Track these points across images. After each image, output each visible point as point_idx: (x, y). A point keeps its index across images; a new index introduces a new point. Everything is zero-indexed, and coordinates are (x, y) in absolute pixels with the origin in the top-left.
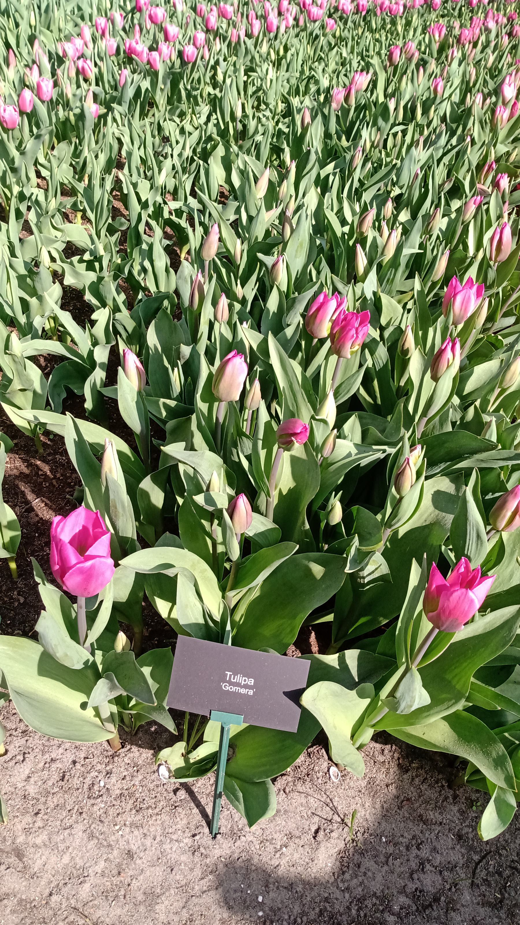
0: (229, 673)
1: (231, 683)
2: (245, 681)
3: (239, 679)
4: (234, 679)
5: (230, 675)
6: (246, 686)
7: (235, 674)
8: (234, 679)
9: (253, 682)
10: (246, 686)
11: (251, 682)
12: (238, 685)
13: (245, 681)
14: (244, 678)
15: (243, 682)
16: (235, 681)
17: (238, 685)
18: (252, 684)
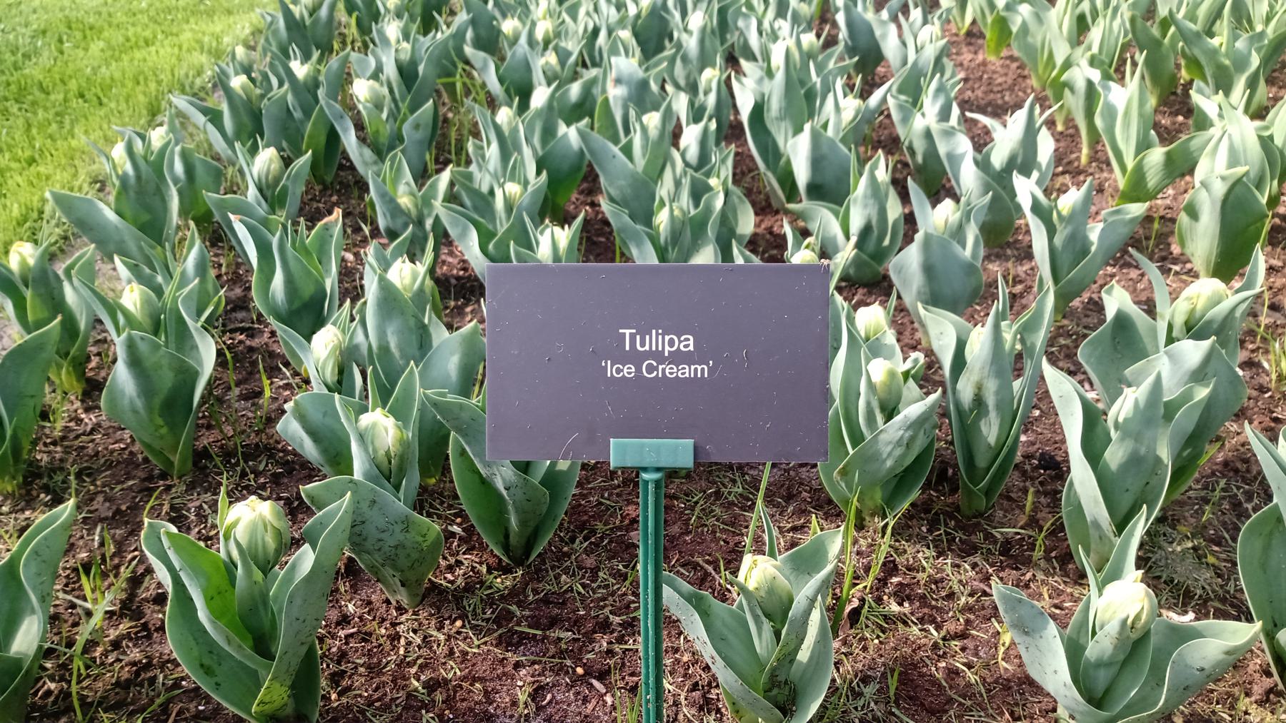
0: (627, 332)
2: (671, 343)
3: (657, 341)
4: (643, 345)
5: (633, 337)
6: (678, 358)
7: (644, 332)
8: (643, 345)
9: (691, 342)
10: (678, 358)
11: (688, 343)
13: (671, 343)
14: (667, 338)
15: (667, 348)
16: (647, 348)
18: (691, 348)
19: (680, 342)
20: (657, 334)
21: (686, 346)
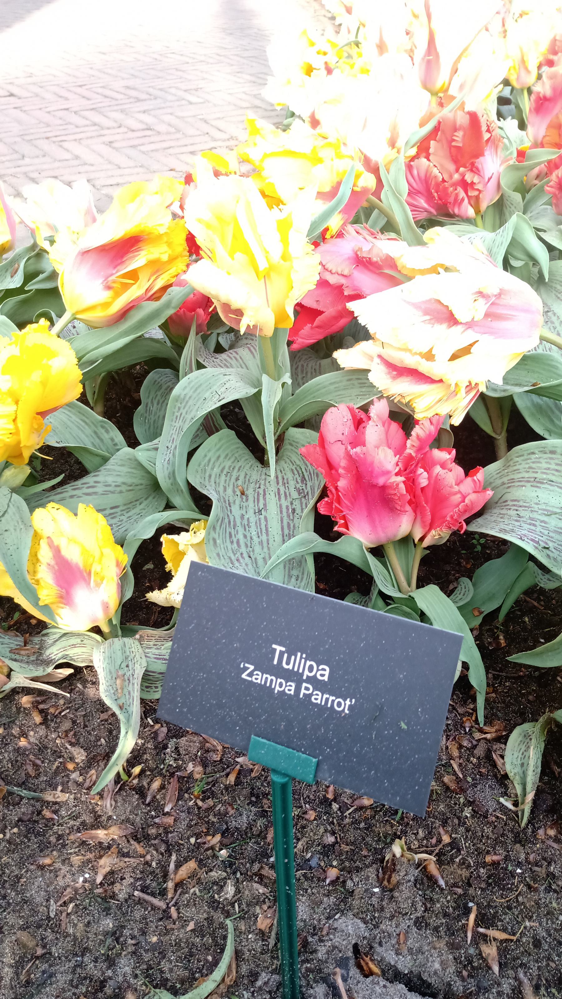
0: (279, 648)
1: (279, 672)
2: (311, 669)
3: (298, 663)
4: (288, 663)
5: (282, 654)
7: (291, 652)
8: (288, 663)
9: (327, 673)
11: (324, 673)
12: (289, 675)
13: (311, 669)
14: (309, 663)
15: (306, 673)
16: (290, 667)
17: (294, 676)
18: (326, 678)
19: (318, 670)
20: (301, 658)
21: (322, 675)
